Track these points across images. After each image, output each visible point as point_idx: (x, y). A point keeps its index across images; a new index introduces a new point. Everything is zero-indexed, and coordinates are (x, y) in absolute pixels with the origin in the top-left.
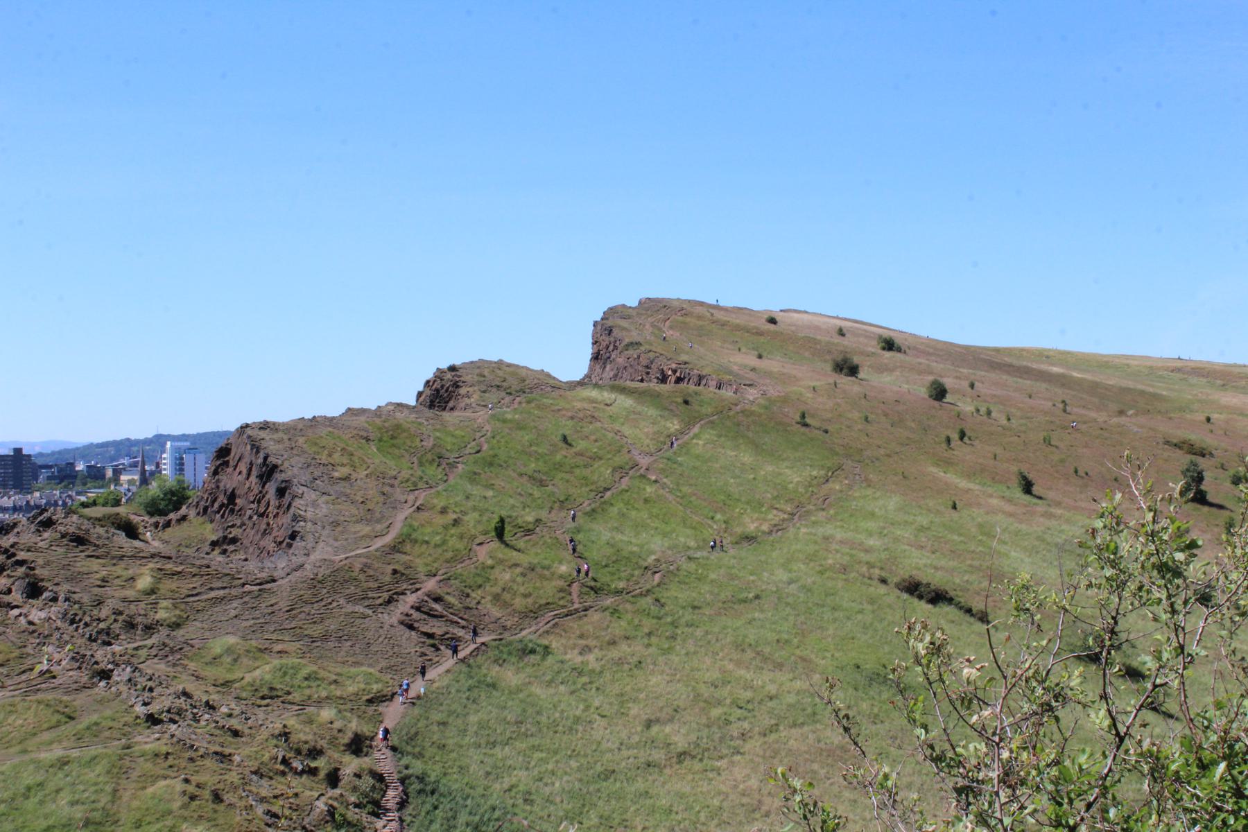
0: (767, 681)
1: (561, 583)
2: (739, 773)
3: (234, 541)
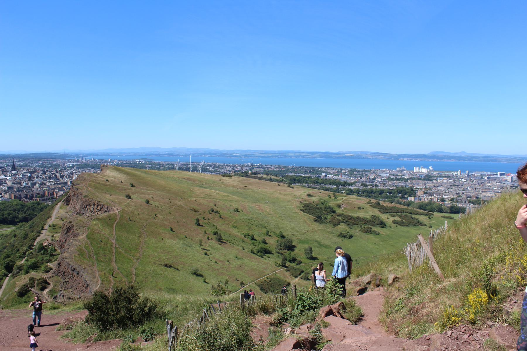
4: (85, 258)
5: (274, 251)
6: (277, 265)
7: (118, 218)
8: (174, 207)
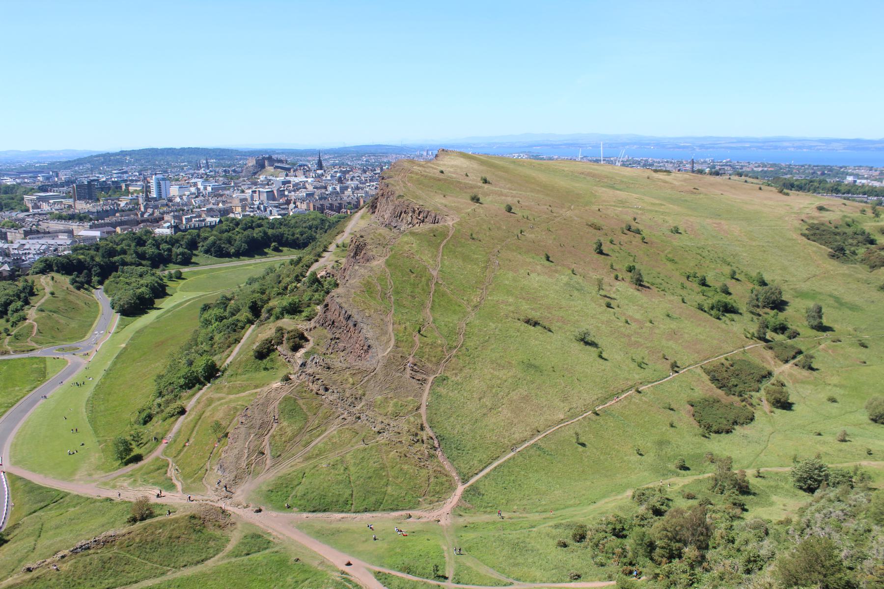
0: (502, 374)
1: (440, 349)
2: (505, 411)
3: (338, 339)
4: (375, 300)
5: (743, 308)
6: (749, 336)
7: (451, 234)
8: (558, 219)
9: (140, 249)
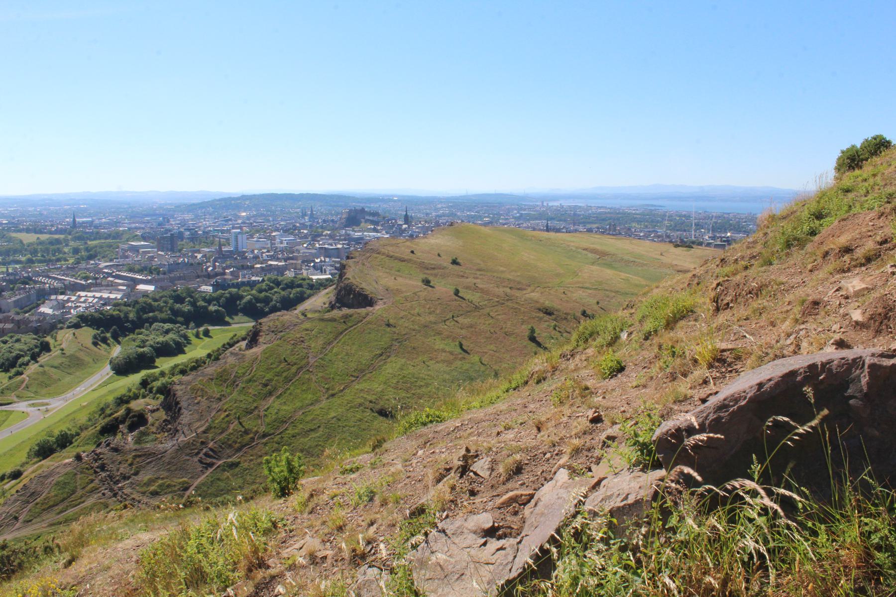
1: (251, 435)
9: (178, 306)
